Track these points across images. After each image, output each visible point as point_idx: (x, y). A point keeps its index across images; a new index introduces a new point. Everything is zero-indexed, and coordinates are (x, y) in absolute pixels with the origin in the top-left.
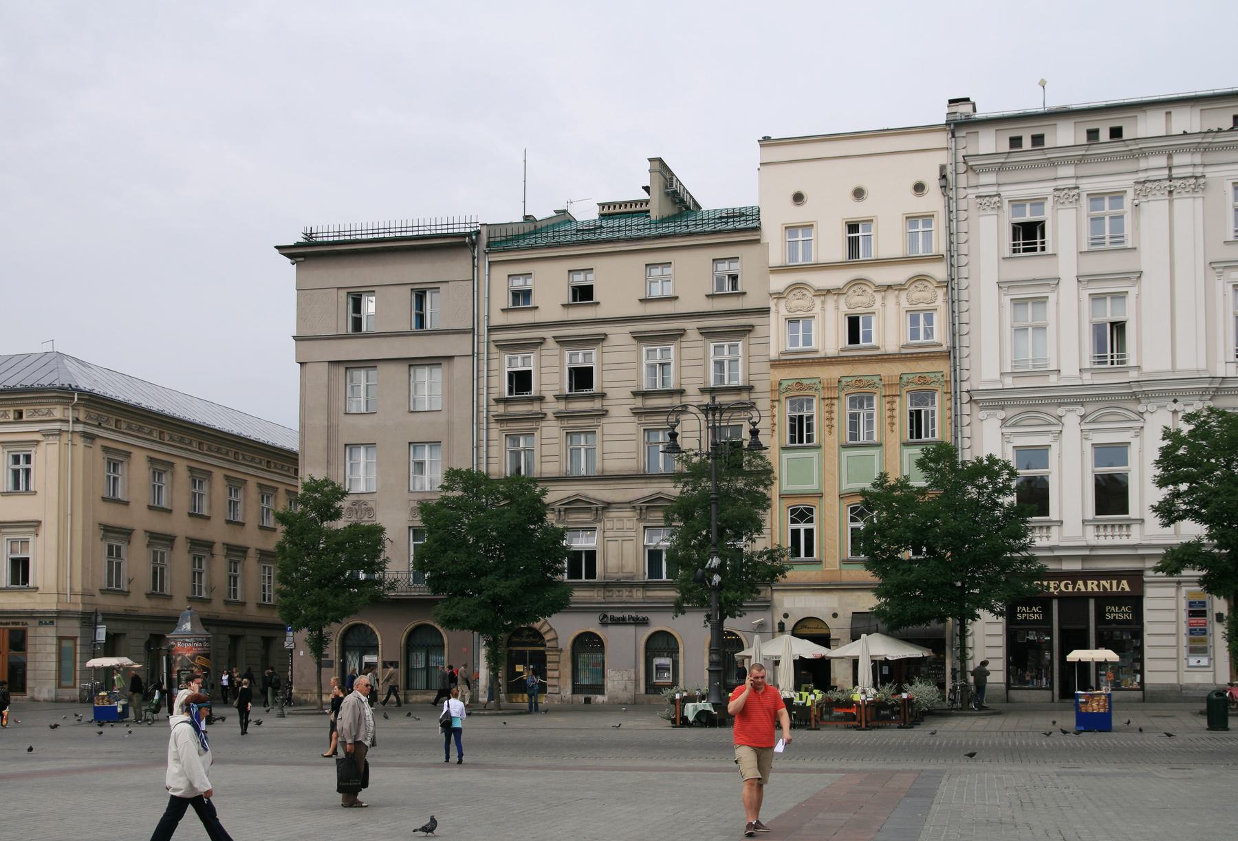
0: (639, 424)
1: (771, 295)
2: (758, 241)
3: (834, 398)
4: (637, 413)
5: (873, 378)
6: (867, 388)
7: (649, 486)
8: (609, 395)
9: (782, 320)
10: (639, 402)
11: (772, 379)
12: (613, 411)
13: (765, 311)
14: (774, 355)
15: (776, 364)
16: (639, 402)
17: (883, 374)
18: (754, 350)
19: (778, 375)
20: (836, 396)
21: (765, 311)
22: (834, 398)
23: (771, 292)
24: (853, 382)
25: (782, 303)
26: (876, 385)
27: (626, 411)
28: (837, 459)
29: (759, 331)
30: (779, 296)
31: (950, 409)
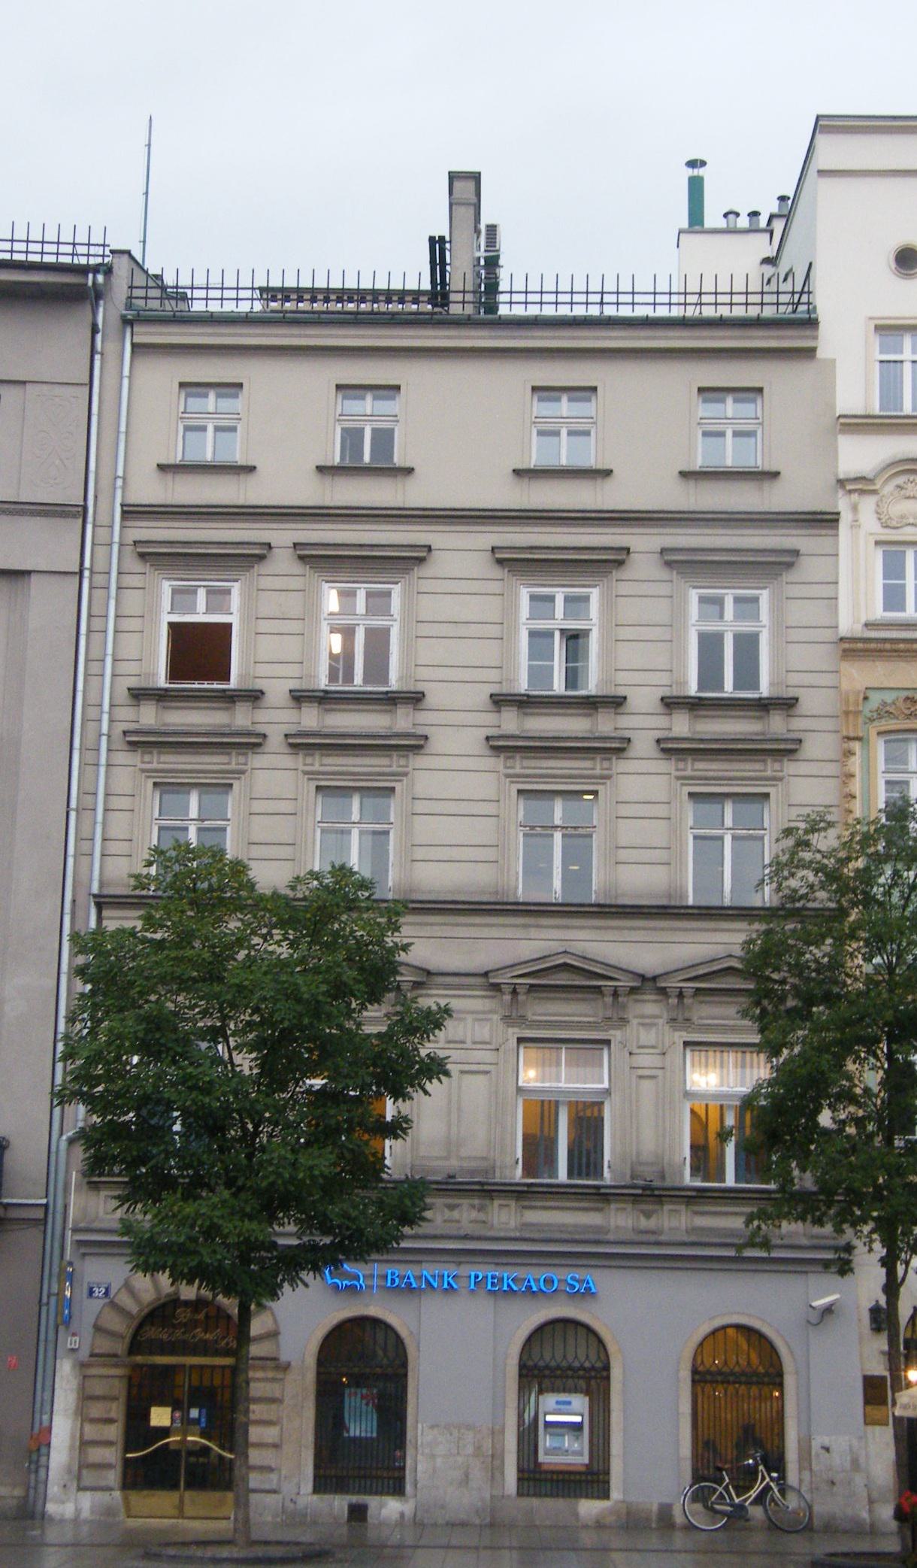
0: (678, 778)
1: (841, 483)
2: (809, 353)
4: (500, 747)
8: (431, 700)
9: (866, 545)
10: (510, 722)
11: (845, 686)
12: (442, 741)
13: (825, 521)
14: (848, 623)
15: (854, 649)
16: (510, 722)
18: (800, 613)
19: (859, 676)
21: (825, 521)
23: (841, 476)
25: (868, 504)
27: (472, 740)
29: (810, 568)
30: (859, 485)
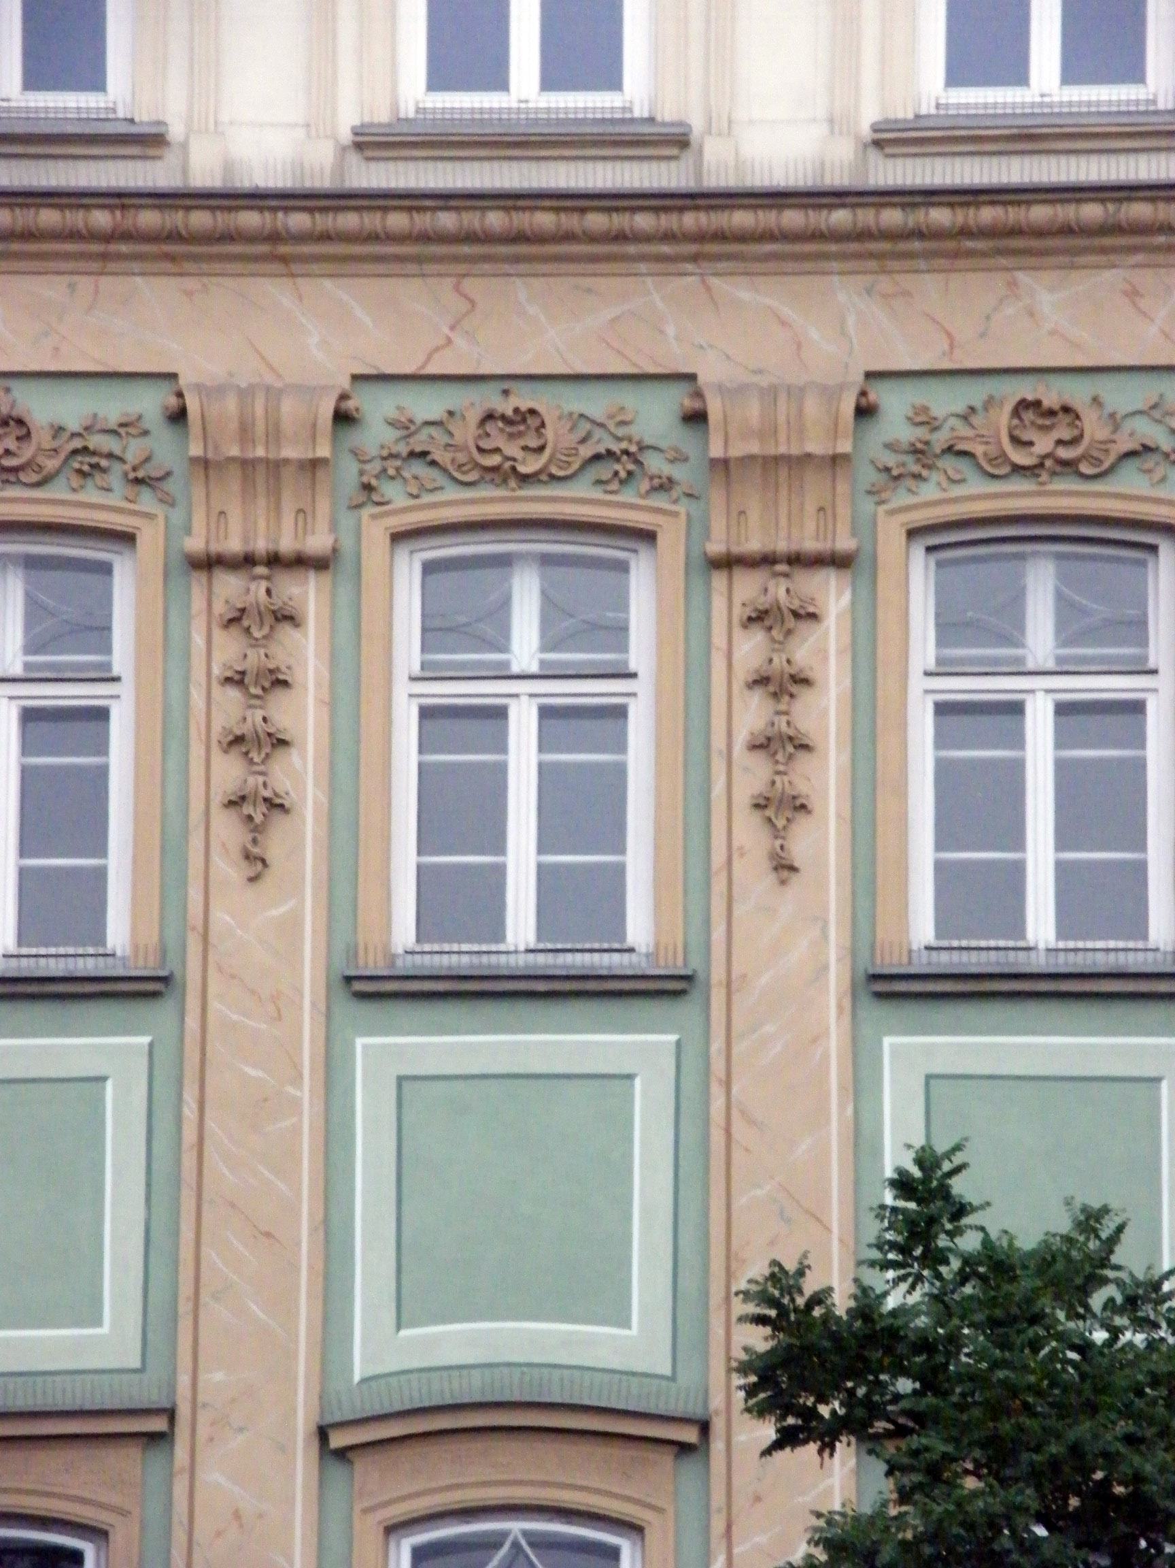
3: (300, 562)
5: (629, 398)
6: (582, 489)
17: (710, 372)
20: (317, 542)
22: (300, 562)
24: (466, 433)
26: (655, 464)
28: (306, 1093)
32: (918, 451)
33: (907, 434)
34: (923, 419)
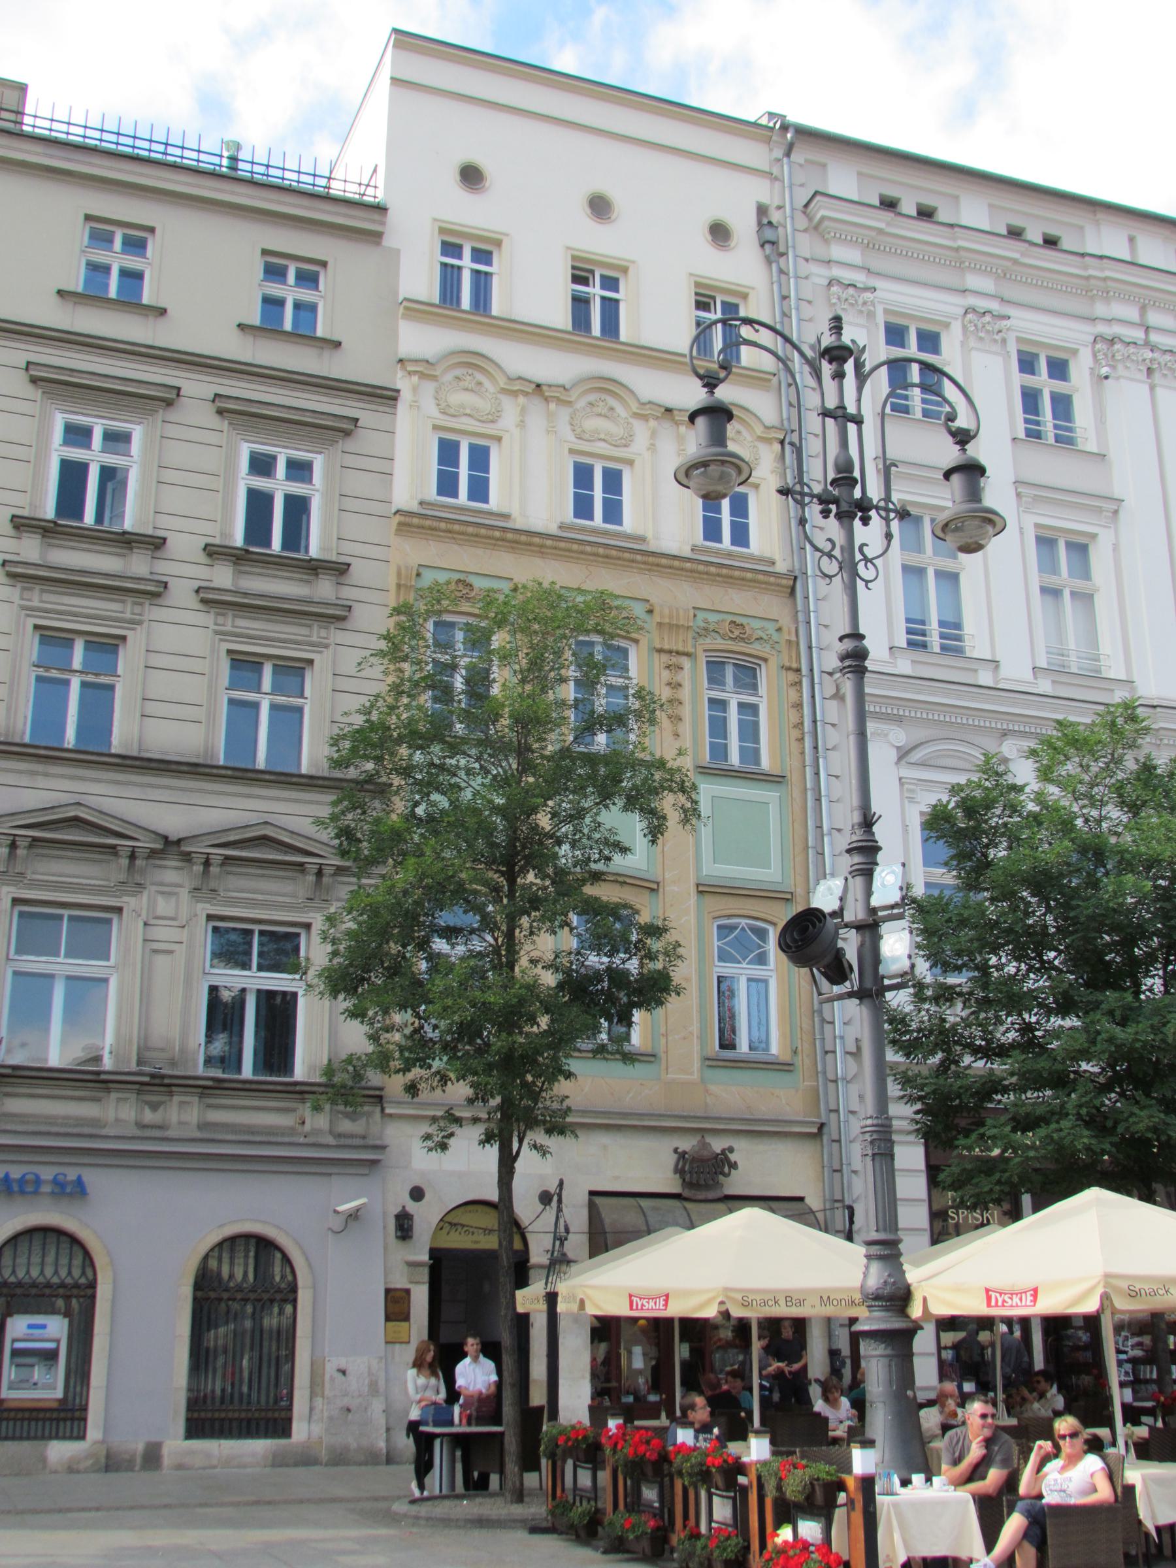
7: (41, 782)
31: (799, 706)
32: (705, 629)
33: (703, 625)
34: (706, 621)
